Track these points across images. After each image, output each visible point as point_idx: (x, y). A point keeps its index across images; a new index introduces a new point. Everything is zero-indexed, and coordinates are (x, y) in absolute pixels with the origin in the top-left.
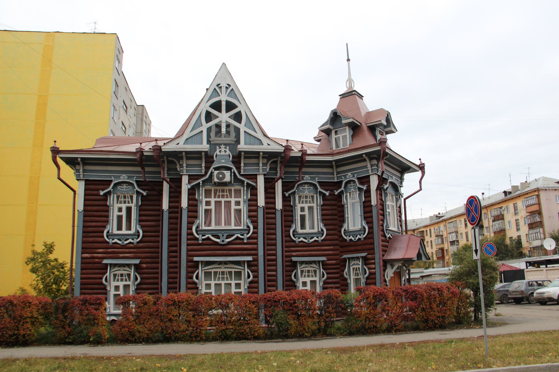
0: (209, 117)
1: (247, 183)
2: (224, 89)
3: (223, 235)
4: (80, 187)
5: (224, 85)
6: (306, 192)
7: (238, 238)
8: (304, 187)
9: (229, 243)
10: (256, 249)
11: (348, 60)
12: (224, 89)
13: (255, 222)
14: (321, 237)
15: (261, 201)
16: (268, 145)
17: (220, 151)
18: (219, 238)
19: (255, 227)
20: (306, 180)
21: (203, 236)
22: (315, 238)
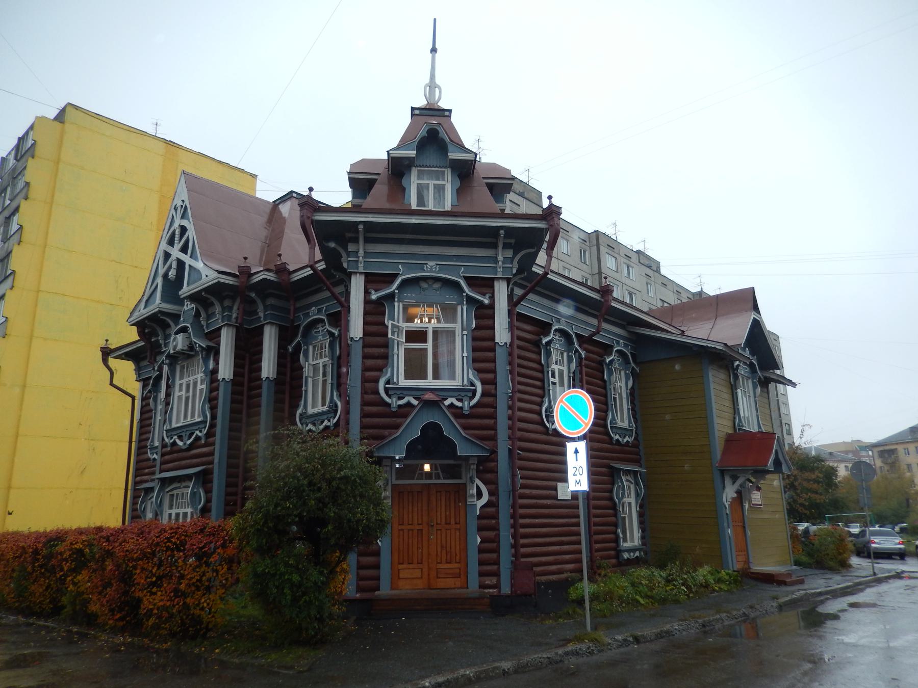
0: (167, 255)
1: (199, 345)
2: (179, 209)
3: (186, 435)
4: (135, 388)
5: (180, 203)
6: (319, 338)
7: (198, 438)
8: (318, 328)
9: (191, 447)
10: (212, 454)
11: (434, 50)
12: (179, 209)
13: (213, 408)
14: (334, 418)
15: (226, 371)
16: (207, 276)
17: (187, 305)
18: (182, 441)
19: (214, 417)
20: (312, 316)
21: (172, 438)
22: (326, 423)
